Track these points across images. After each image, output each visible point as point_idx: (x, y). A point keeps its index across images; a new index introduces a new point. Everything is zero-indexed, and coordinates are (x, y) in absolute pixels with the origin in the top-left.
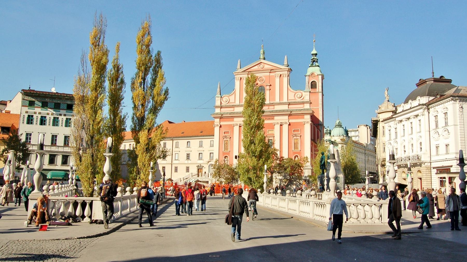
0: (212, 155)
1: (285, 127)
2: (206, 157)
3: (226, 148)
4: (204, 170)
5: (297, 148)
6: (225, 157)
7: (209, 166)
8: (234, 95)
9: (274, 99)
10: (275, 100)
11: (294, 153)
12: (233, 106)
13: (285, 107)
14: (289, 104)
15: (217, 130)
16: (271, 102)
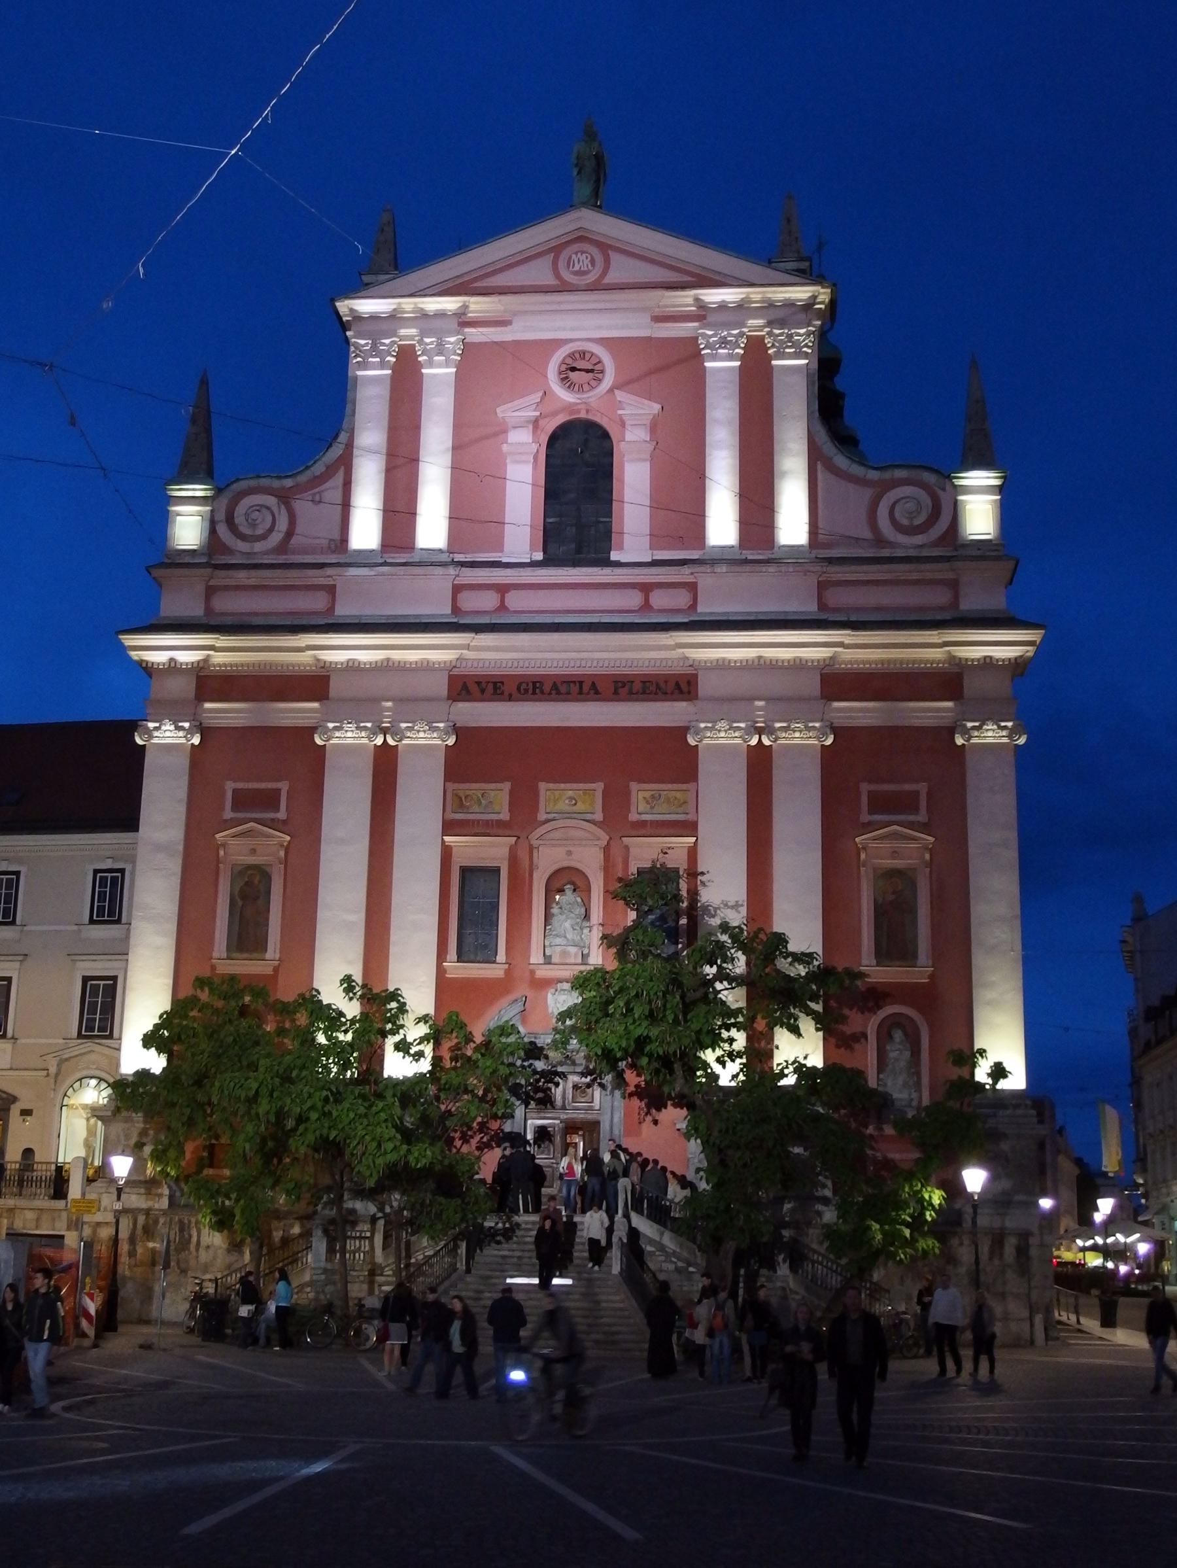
3: (248, 936)
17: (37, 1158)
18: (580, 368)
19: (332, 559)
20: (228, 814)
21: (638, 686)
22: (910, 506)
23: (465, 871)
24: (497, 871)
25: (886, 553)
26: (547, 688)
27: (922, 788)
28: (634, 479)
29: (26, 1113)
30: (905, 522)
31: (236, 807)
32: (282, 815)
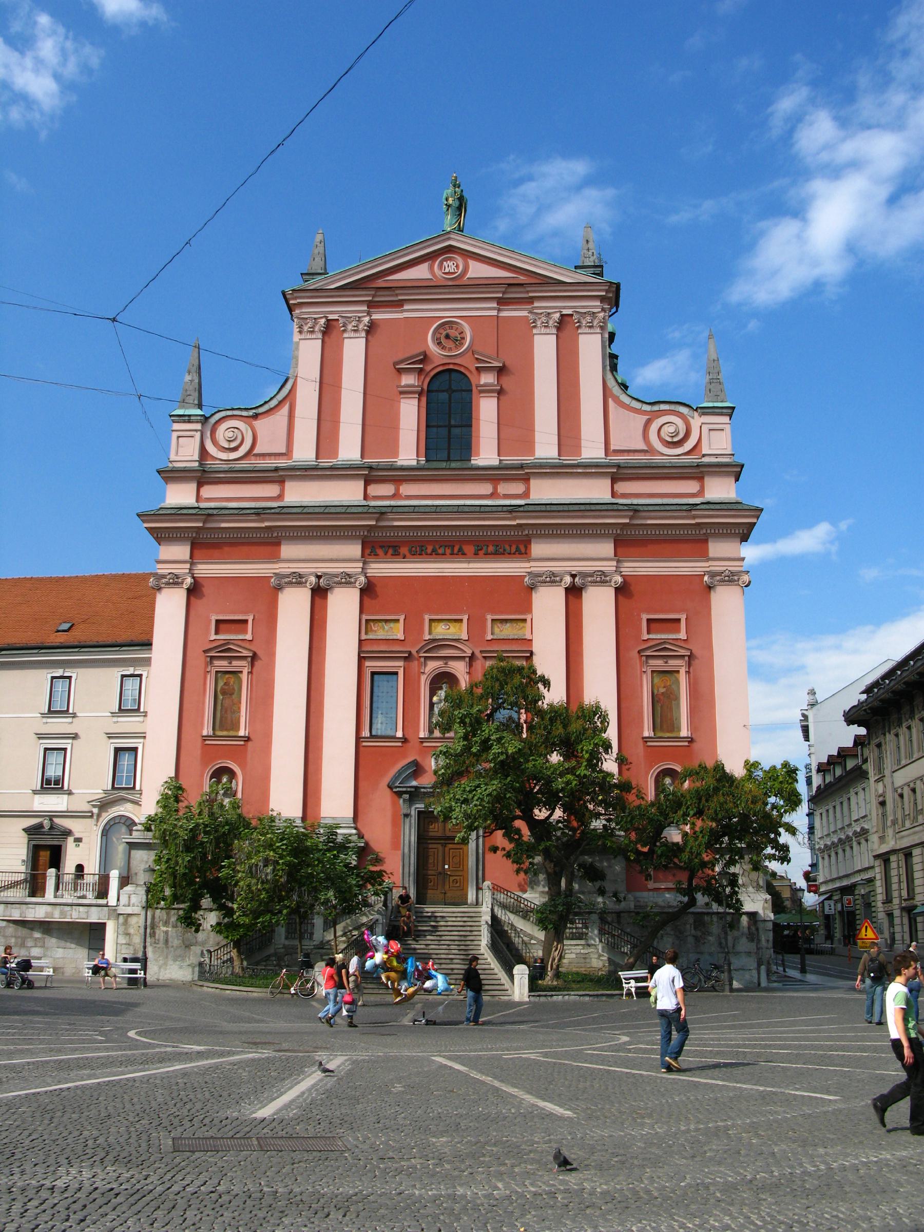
0: (126, 760)
1: (599, 606)
2: (89, 775)
3: (225, 718)
4: (72, 856)
5: (674, 726)
6: (218, 774)
7: (105, 833)
8: (285, 410)
9: (529, 444)
10: (531, 450)
11: (654, 754)
12: (279, 476)
13: (597, 491)
14: (618, 473)
15: (169, 610)
16: (510, 459)
17: (86, 871)
18: (448, 334)
19: (282, 463)
20: (213, 637)
21: (491, 549)
22: (672, 429)
23: (373, 674)
24: (396, 673)
25: (657, 459)
26: (429, 551)
27: (683, 617)
28: (487, 411)
29: (78, 840)
30: (669, 440)
31: (217, 633)
32: (249, 637)
